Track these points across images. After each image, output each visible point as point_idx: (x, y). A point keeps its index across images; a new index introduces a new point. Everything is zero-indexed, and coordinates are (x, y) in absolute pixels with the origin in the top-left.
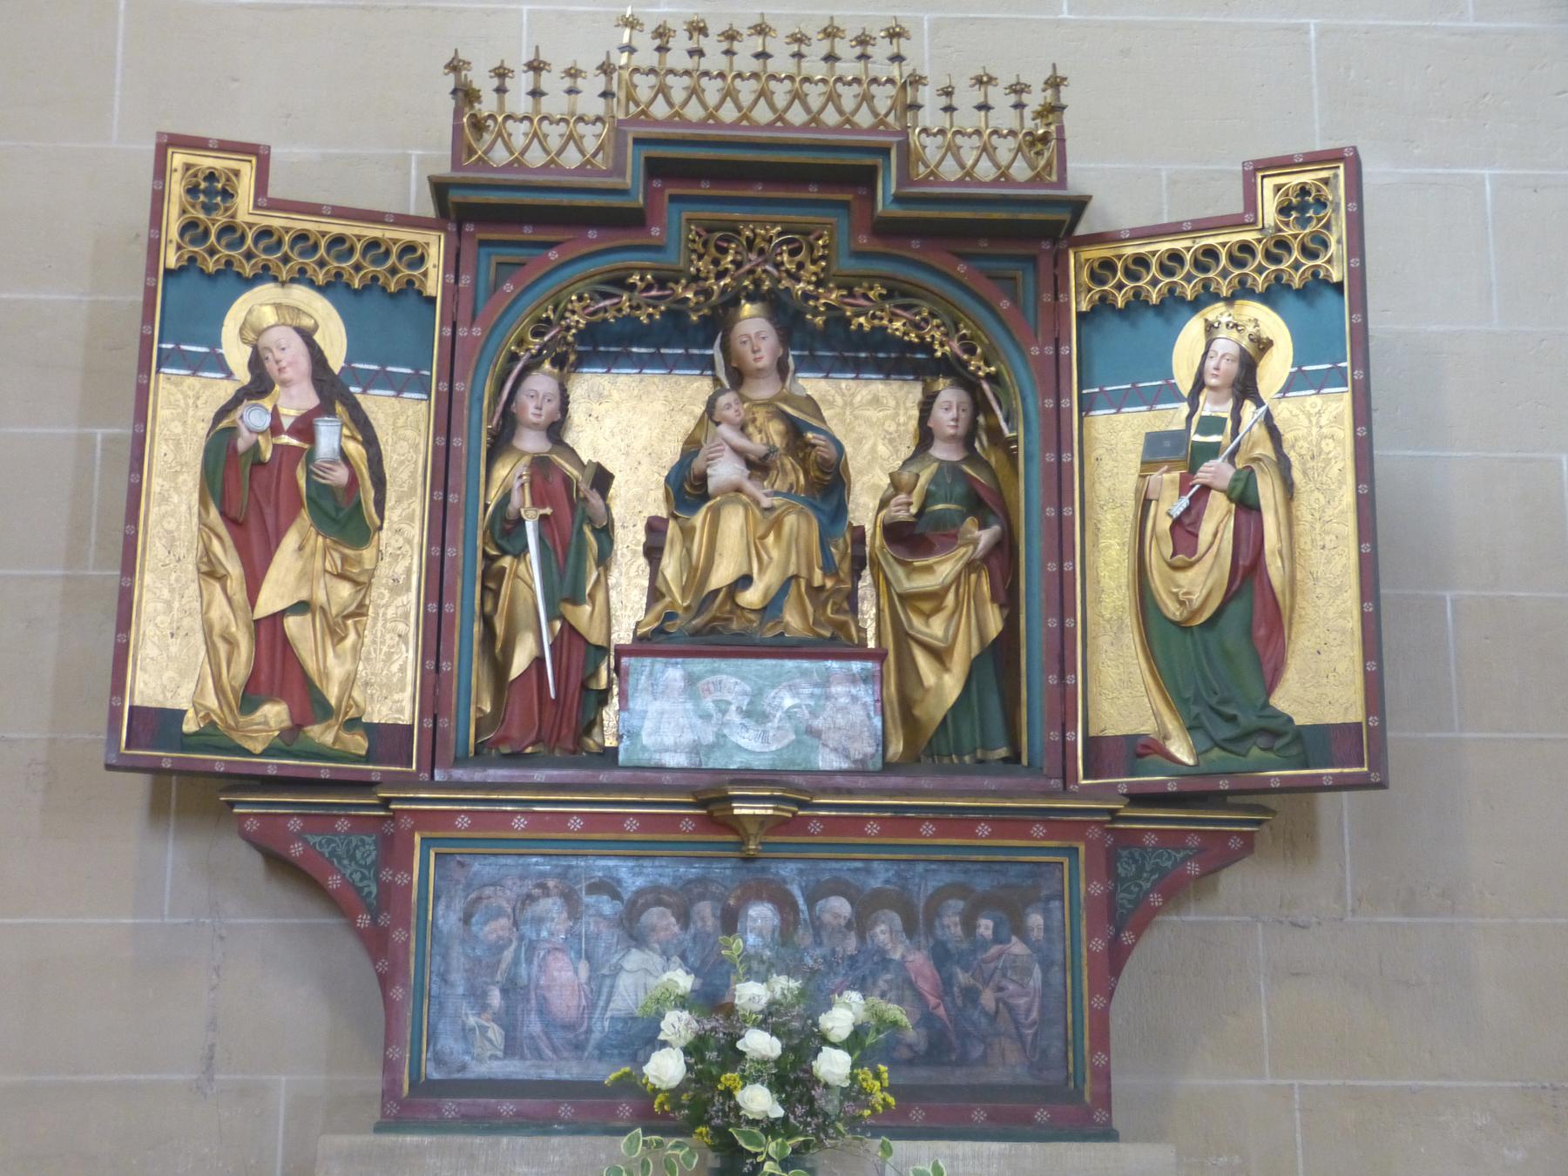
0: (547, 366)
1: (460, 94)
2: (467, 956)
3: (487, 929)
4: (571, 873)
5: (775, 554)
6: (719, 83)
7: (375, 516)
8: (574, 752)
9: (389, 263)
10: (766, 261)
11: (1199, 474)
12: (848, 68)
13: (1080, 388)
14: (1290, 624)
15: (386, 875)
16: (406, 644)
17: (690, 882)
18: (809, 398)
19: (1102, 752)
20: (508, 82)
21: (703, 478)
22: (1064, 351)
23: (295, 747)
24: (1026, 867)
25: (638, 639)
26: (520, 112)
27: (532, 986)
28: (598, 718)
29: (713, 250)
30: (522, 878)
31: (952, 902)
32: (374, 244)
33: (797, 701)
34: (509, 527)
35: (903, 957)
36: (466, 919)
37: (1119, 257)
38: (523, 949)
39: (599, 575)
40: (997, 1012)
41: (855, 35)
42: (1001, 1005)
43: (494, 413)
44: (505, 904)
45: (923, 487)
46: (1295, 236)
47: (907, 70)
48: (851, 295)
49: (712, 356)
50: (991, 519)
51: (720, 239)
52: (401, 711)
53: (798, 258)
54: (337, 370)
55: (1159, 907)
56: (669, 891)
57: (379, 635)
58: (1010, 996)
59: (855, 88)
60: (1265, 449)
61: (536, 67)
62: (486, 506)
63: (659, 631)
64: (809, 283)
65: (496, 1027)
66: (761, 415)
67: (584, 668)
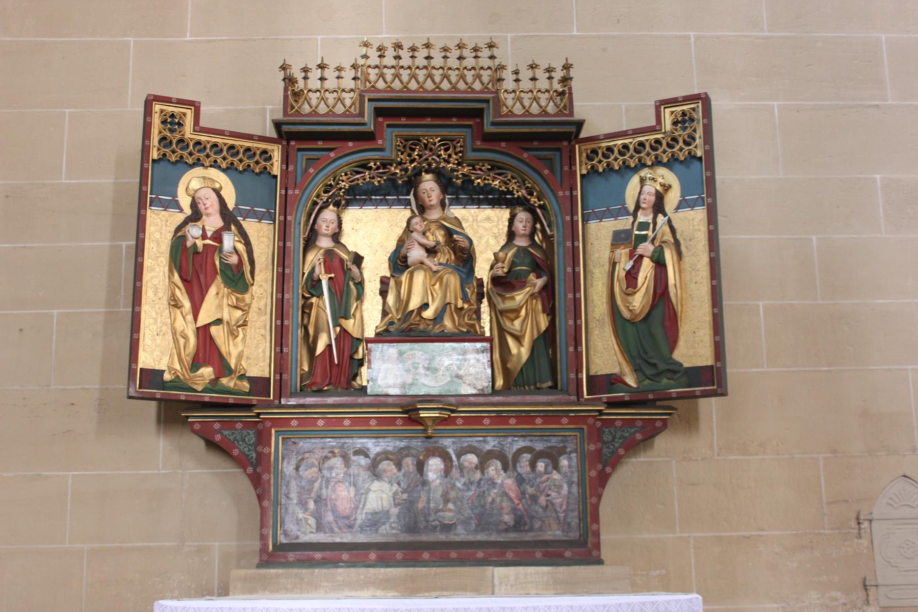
0: (331, 207)
1: (287, 81)
2: (297, 485)
3: (307, 473)
4: (346, 446)
5: (439, 292)
6: (408, 71)
7: (250, 279)
8: (347, 389)
9: (255, 159)
10: (433, 154)
11: (638, 250)
12: (470, 62)
13: (583, 210)
14: (681, 320)
15: (260, 449)
16: (265, 339)
17: (402, 449)
18: (456, 218)
19: (599, 383)
20: (309, 74)
21: (405, 258)
22: (574, 193)
23: (216, 388)
24: (560, 438)
25: (377, 334)
26: (314, 88)
27: (328, 499)
29: (408, 150)
30: (323, 448)
31: (525, 455)
32: (248, 149)
33: (451, 362)
35: (502, 481)
36: (297, 468)
37: (599, 148)
38: (324, 482)
39: (357, 305)
40: (547, 506)
41: (473, 47)
42: (548, 503)
43: (306, 230)
44: (315, 461)
45: (510, 259)
46: (680, 136)
47: (497, 64)
48: (474, 169)
49: (409, 199)
50: (543, 273)
51: (412, 144)
52: (263, 371)
53: (449, 152)
54: (231, 209)
55: (623, 455)
56: (392, 453)
57: (253, 335)
58: (554, 499)
59: (473, 72)
60: (669, 237)
61: (322, 67)
62: (304, 274)
63: (386, 330)
64: (454, 164)
65: (312, 518)
66: (433, 227)
67: (351, 349)
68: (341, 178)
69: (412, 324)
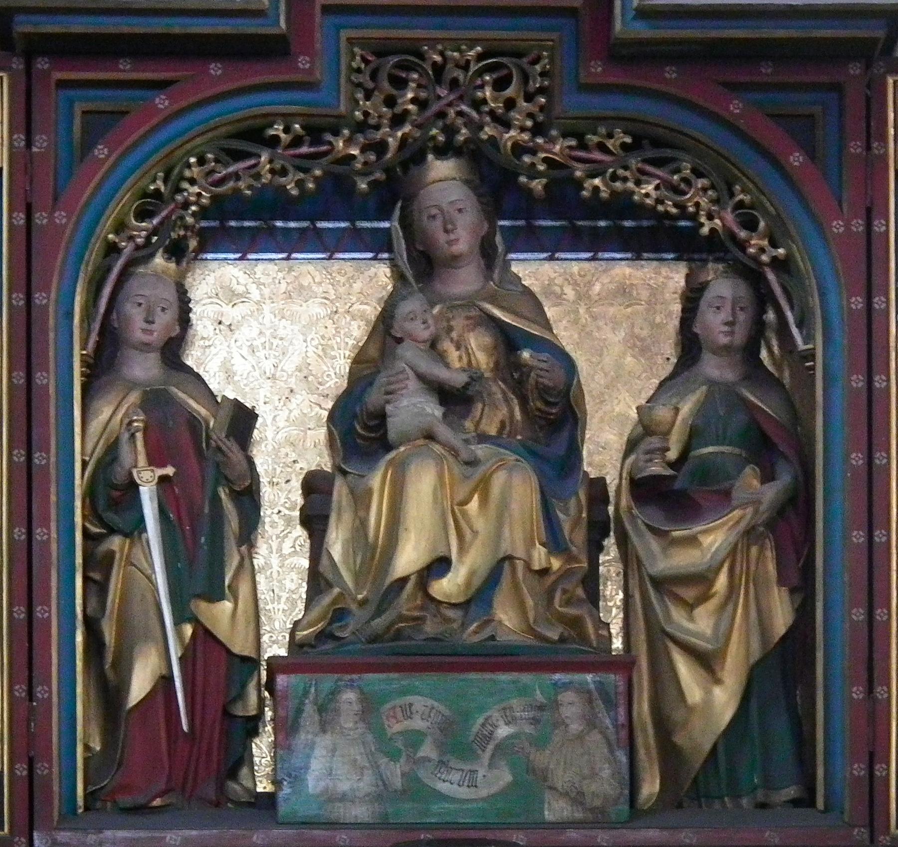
10: (461, 98)
21: (381, 417)
28: (246, 755)
29: (386, 85)
34: (116, 494)
48: (583, 145)
51: (400, 66)
53: (510, 92)
64: (523, 129)
68: (187, 173)
69: (401, 618)
